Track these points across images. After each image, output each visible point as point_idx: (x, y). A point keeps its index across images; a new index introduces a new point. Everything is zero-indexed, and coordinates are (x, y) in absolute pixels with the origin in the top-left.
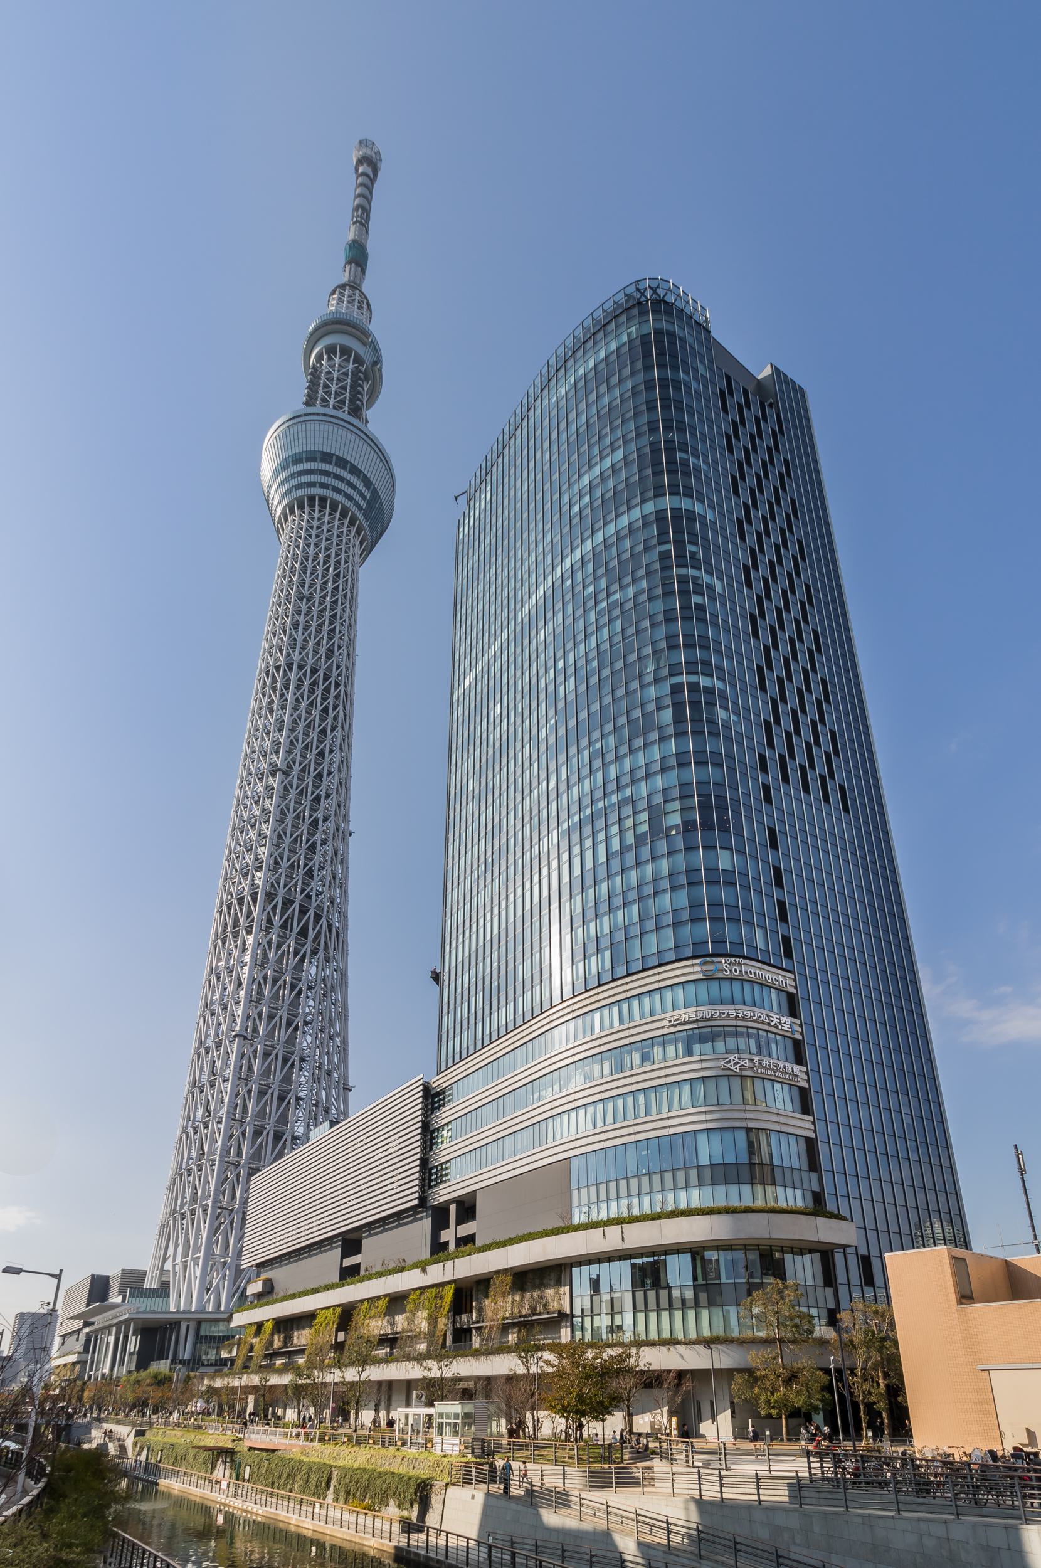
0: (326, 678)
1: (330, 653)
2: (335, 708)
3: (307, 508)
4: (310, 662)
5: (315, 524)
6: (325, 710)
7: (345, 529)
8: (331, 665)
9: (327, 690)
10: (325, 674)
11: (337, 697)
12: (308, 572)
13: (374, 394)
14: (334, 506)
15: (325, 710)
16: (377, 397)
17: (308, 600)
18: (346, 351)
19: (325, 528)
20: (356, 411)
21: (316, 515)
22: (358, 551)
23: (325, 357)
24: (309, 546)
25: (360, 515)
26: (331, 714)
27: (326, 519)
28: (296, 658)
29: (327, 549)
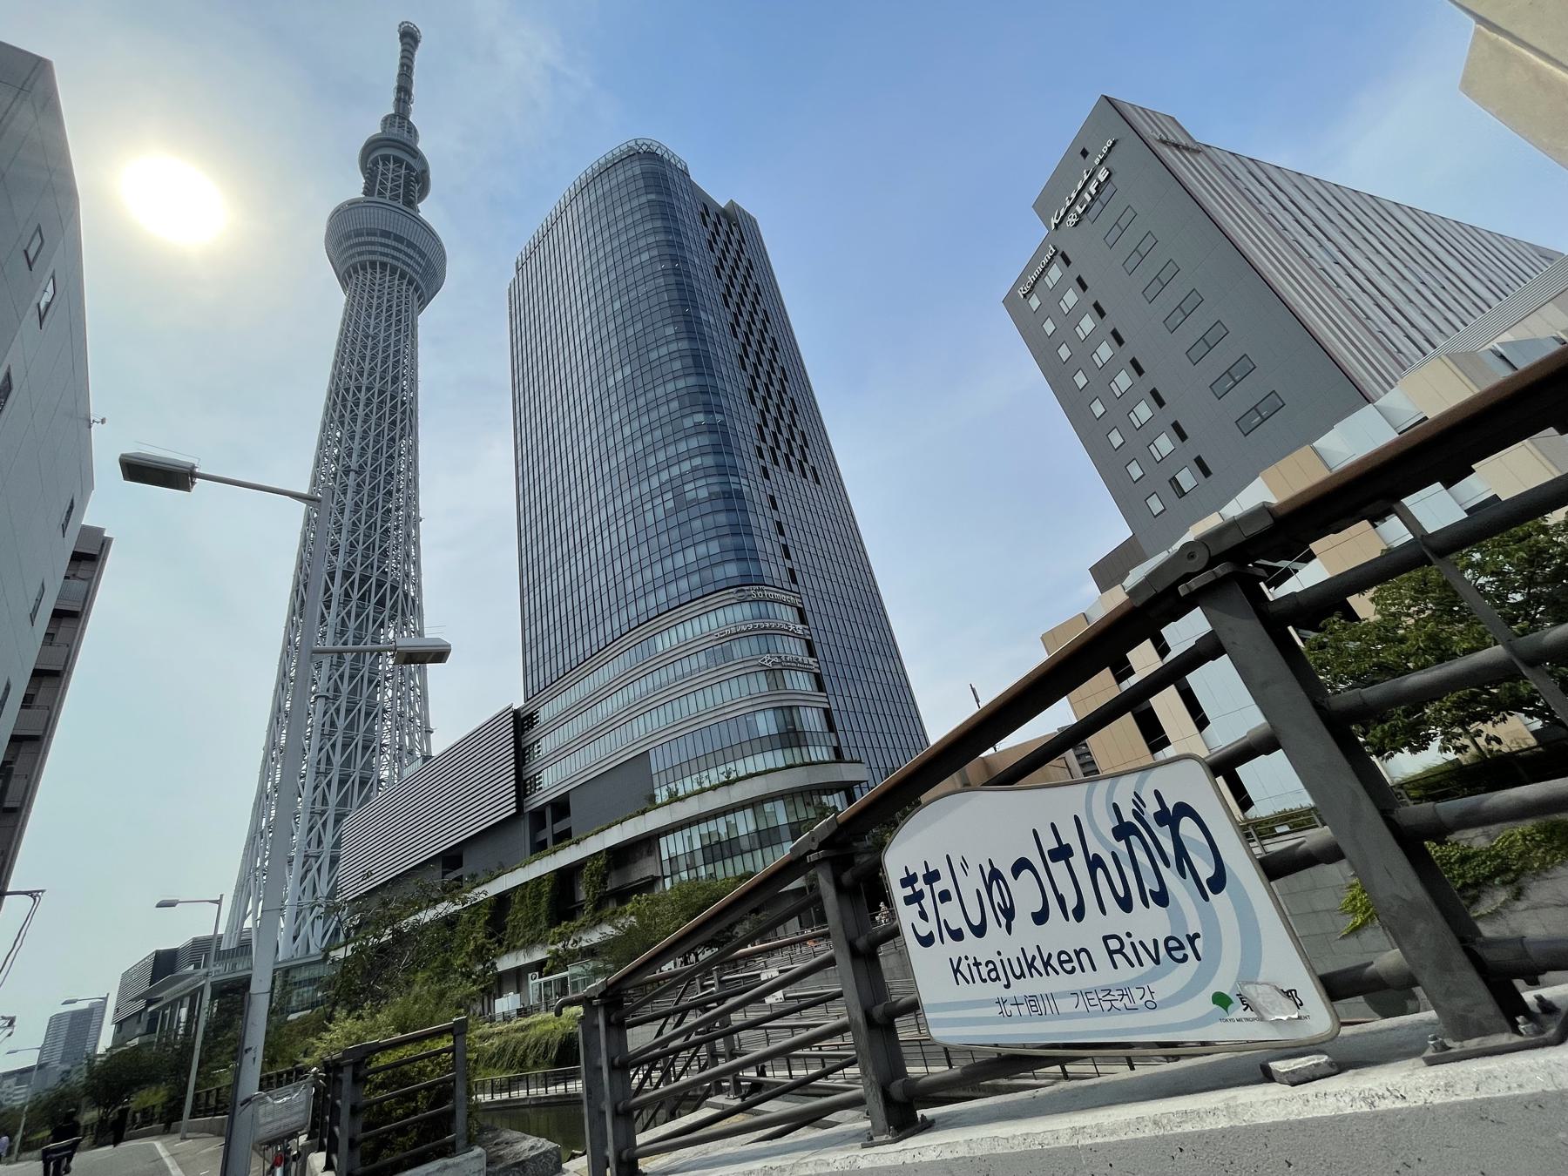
1: (395, 380)
2: (402, 421)
3: (369, 270)
4: (377, 386)
6: (394, 423)
7: (404, 287)
8: (397, 388)
9: (394, 407)
11: (404, 413)
12: (373, 317)
13: (424, 191)
14: (394, 270)
15: (394, 423)
16: (426, 195)
17: (373, 339)
18: (398, 160)
19: (386, 285)
20: (410, 203)
21: (378, 276)
22: (416, 303)
23: (381, 163)
25: (417, 277)
26: (399, 427)
27: (387, 278)
28: (364, 381)
29: (388, 301)
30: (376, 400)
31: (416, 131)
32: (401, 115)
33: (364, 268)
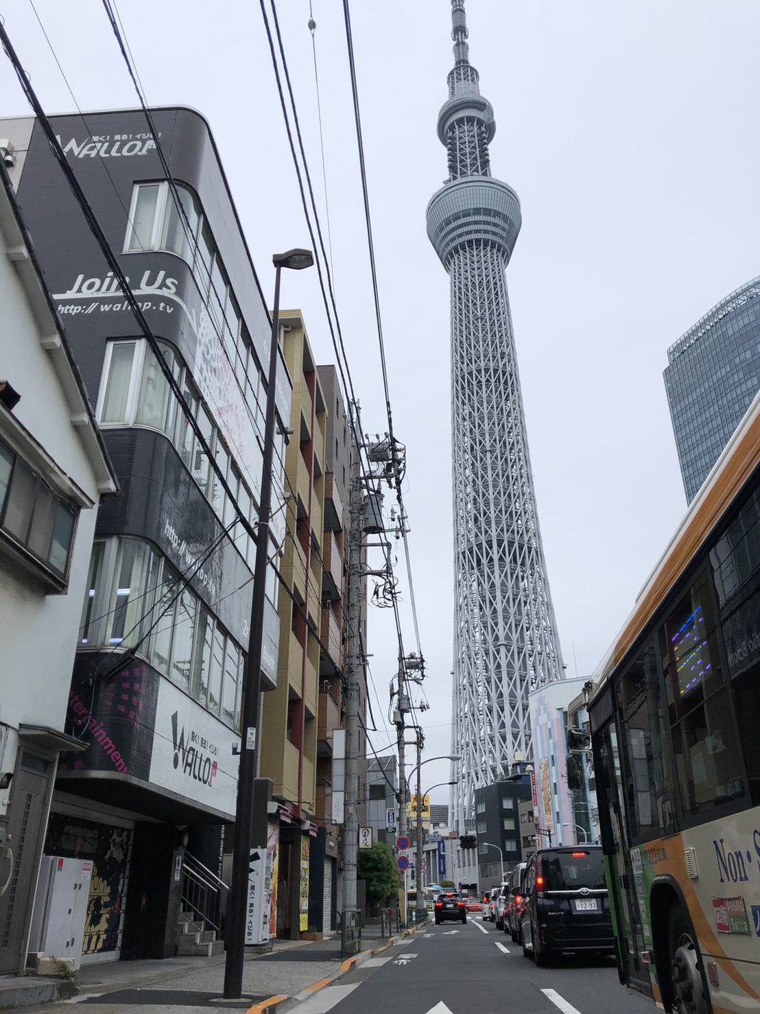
0: (504, 373)
3: (467, 249)
5: (475, 259)
10: (503, 371)
14: (486, 242)
18: (470, 120)
24: (474, 276)
27: (482, 254)
28: (482, 365)
30: (493, 380)
31: (477, 73)
32: (463, 70)
33: (463, 249)
